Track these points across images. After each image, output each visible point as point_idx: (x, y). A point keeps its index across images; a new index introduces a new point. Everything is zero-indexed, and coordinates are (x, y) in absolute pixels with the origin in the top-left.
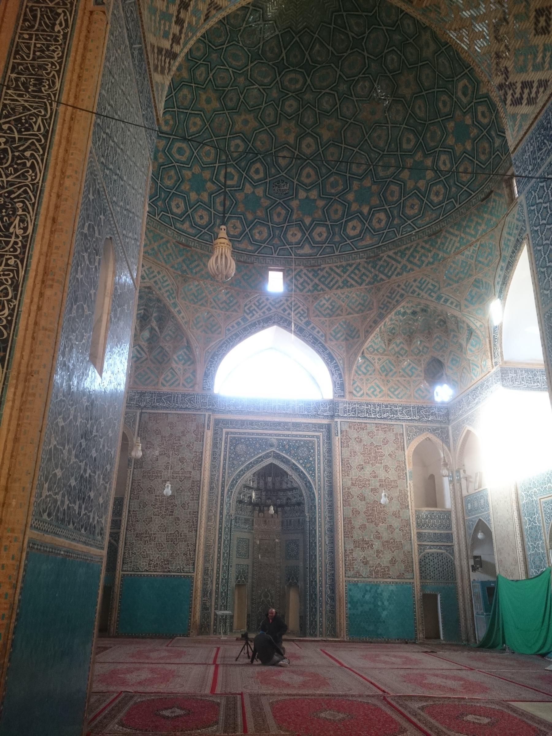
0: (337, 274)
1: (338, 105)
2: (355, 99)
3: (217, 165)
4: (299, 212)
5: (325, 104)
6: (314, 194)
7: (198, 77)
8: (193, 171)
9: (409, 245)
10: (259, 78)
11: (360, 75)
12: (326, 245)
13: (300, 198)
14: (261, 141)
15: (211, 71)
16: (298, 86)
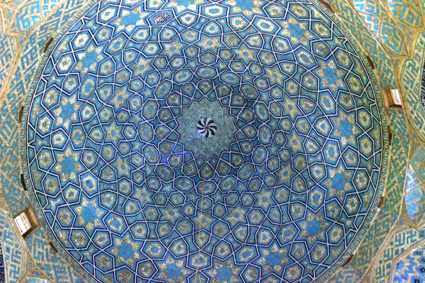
0: (71, 10)
1: (144, 82)
2: (136, 93)
3: (228, 16)
4: (137, 13)
5: (154, 77)
6: (129, 29)
7: (258, 68)
8: (251, 13)
9: (30, 85)
10: (208, 70)
11: (142, 108)
12: (97, 14)
13: (141, 20)
14: (192, 36)
15: (248, 70)
16: (178, 75)
